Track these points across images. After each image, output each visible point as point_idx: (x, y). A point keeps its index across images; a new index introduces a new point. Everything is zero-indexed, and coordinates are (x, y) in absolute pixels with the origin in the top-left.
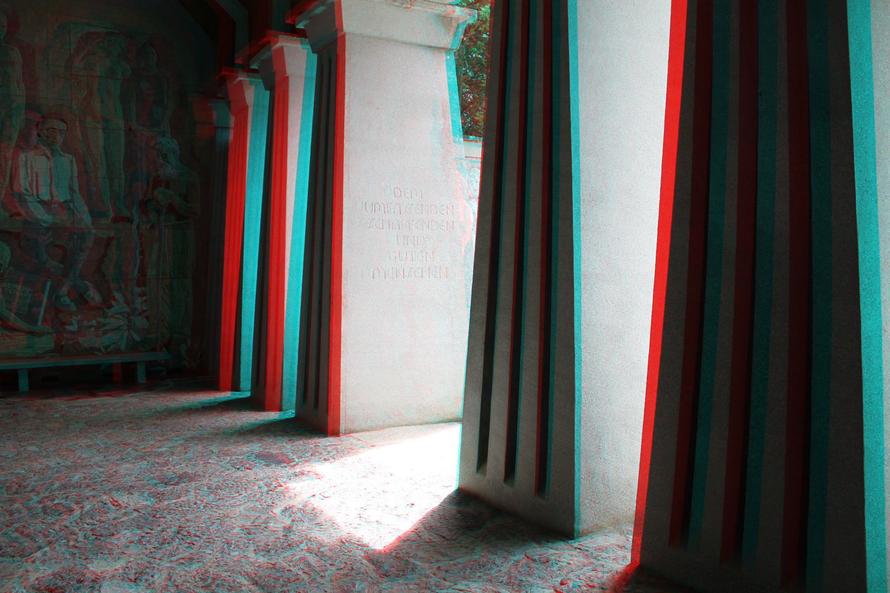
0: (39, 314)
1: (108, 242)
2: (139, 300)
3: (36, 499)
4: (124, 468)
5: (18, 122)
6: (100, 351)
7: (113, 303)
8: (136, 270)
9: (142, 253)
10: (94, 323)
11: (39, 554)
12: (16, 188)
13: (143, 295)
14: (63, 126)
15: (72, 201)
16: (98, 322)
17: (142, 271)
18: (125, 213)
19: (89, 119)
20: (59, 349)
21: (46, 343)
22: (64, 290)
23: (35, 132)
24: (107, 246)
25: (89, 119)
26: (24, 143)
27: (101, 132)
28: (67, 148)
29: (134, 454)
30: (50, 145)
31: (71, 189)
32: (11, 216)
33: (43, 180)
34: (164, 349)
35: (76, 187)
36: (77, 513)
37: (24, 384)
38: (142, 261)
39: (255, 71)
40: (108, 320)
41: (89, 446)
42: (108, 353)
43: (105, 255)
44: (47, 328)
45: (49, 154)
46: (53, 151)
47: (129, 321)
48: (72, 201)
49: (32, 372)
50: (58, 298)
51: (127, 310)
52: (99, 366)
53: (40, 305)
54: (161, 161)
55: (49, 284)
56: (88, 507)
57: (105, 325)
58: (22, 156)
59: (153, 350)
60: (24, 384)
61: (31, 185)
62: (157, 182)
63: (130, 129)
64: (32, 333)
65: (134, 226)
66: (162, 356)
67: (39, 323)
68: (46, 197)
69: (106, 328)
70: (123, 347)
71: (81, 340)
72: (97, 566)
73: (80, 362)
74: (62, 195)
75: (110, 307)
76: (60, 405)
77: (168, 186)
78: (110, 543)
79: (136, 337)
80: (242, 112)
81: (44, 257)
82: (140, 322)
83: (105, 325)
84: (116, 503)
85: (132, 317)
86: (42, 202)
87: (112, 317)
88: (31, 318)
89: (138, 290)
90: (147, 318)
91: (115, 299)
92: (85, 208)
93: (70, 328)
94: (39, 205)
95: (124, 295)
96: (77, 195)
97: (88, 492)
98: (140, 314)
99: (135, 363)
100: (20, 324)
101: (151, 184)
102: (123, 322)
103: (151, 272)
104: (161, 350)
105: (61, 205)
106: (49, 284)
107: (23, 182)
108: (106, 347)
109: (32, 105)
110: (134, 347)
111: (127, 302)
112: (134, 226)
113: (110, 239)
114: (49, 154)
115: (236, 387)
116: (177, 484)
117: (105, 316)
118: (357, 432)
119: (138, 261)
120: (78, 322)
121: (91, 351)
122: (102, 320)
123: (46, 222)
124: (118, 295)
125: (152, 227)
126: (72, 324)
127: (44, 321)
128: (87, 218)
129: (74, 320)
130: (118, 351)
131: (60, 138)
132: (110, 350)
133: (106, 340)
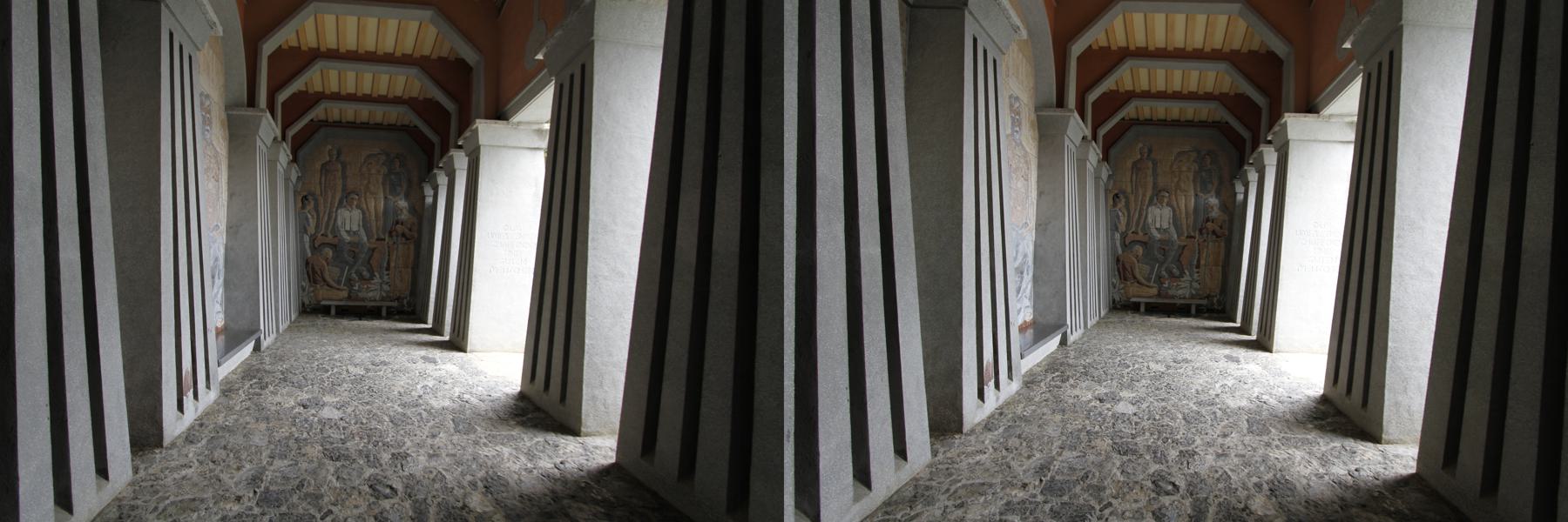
5: (338, 196)
26: (340, 204)
74: (355, 228)
109: (344, 188)
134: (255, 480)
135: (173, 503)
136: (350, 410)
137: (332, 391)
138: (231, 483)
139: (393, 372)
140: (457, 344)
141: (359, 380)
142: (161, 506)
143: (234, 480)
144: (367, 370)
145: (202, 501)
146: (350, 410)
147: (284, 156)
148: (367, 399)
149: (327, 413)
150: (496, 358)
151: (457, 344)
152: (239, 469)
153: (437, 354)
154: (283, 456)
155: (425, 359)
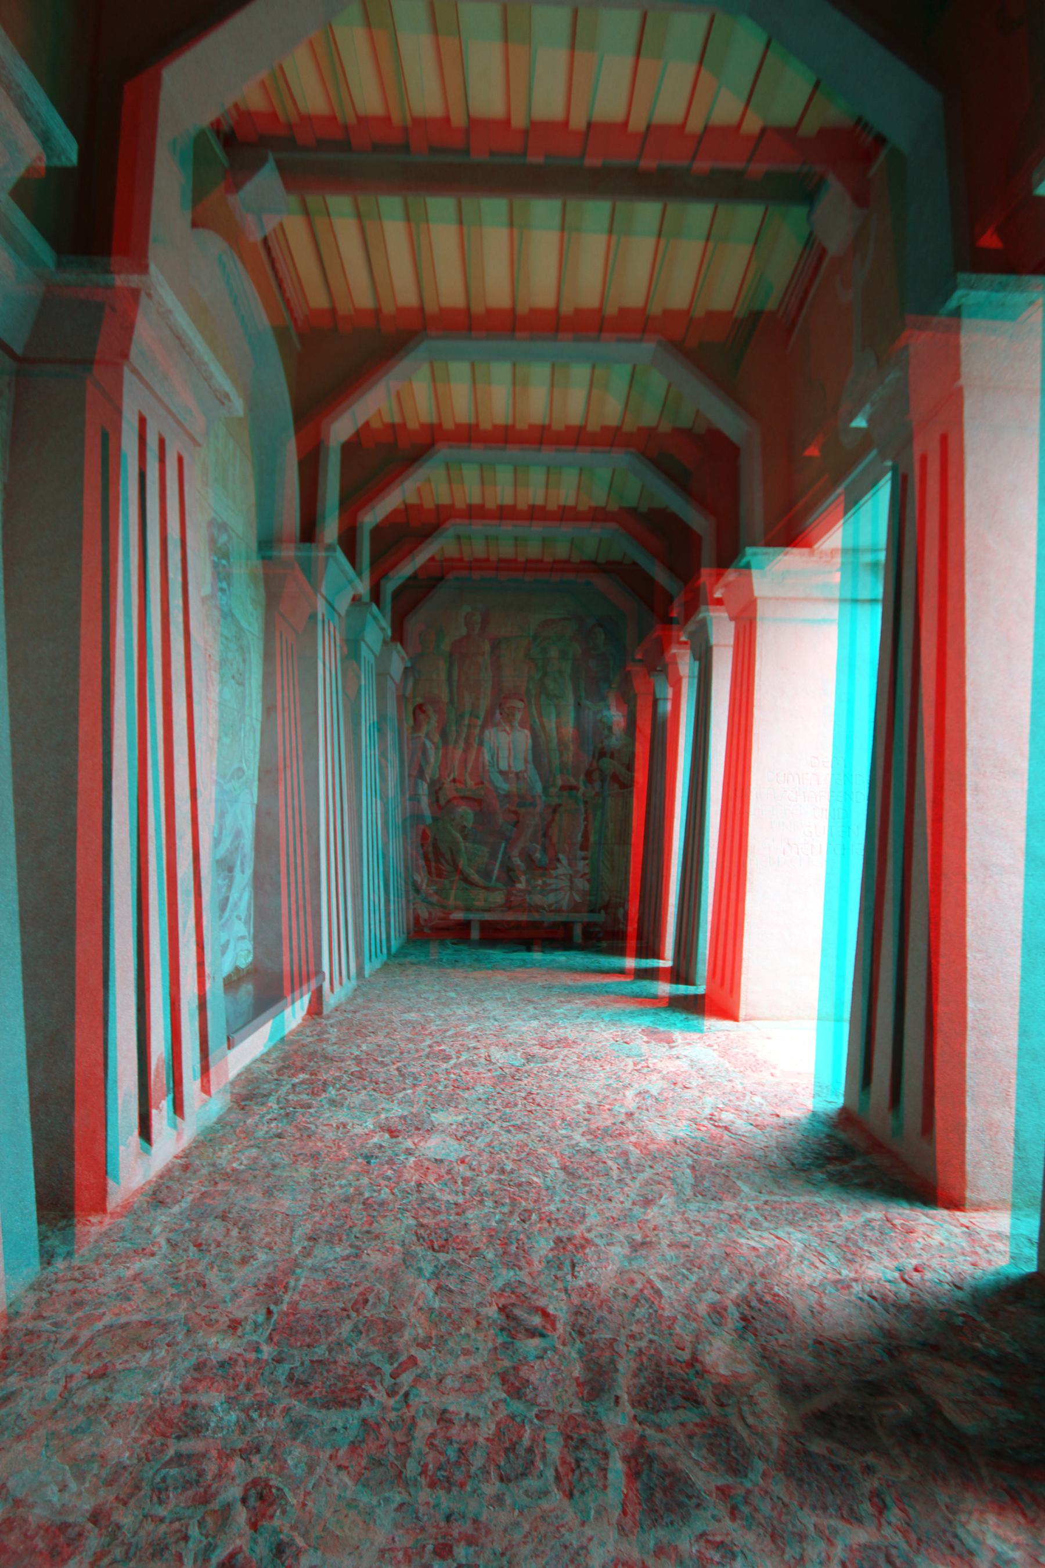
0: (493, 871)
1: (555, 810)
2: (581, 865)
3: (428, 1042)
4: (516, 1024)
5: (485, 703)
6: (544, 908)
7: (558, 865)
8: (580, 835)
9: (586, 819)
10: (540, 882)
11: (400, 1095)
12: (481, 760)
13: (585, 858)
14: (521, 705)
15: (526, 771)
16: (544, 882)
17: (586, 836)
18: (572, 781)
19: (543, 697)
20: (508, 906)
21: (498, 898)
22: (515, 852)
23: (498, 712)
24: (555, 811)
25: (543, 697)
26: (489, 721)
27: (553, 711)
28: (522, 725)
29: (532, 1011)
30: (510, 722)
31: (526, 761)
32: (476, 784)
33: (504, 753)
34: (603, 911)
35: (530, 758)
36: (452, 1062)
37: (475, 934)
38: (586, 827)
39: (685, 643)
40: (552, 881)
41: (498, 999)
42: (551, 911)
43: (553, 820)
44: (500, 885)
45: (508, 729)
46: (512, 727)
47: (571, 882)
48: (526, 771)
49: (484, 925)
50: (509, 858)
51: (571, 872)
52: (542, 923)
53: (494, 865)
54: (606, 732)
55: (503, 845)
56: (464, 1056)
57: (550, 884)
58: (487, 733)
59: (592, 911)
60: (475, 934)
61: (492, 758)
62: (602, 754)
63: (579, 704)
64: (486, 888)
65: (580, 794)
66: (600, 917)
67: (494, 878)
68: (503, 766)
69: (549, 888)
70: (565, 908)
71: (527, 897)
72: (441, 1118)
73: (524, 917)
74: (519, 766)
75: (556, 868)
76: (497, 955)
77: (612, 757)
78: (462, 1097)
79: (577, 898)
80: (677, 685)
81: (501, 821)
82: (582, 884)
83: (550, 884)
84: (488, 1059)
85: (576, 880)
86: (501, 772)
87: (556, 877)
88: (486, 874)
89: (580, 854)
90: (588, 881)
91: (558, 860)
92: (537, 777)
93: (519, 886)
94: (498, 775)
95: (569, 860)
96: (531, 766)
97: (473, 1044)
98: (582, 877)
99: (573, 923)
100: (476, 878)
101: (597, 754)
102: (567, 883)
103: (593, 838)
104: (599, 912)
105: (517, 774)
106: (503, 845)
107: (487, 757)
108: (550, 905)
110: (575, 908)
111: (570, 865)
112: (580, 794)
113: (559, 805)
114: (508, 729)
115: (658, 955)
116: (552, 1048)
117: (550, 876)
118: (759, 1019)
119: (582, 827)
120: (527, 881)
121: (537, 908)
122: (548, 881)
123: (503, 790)
124: (561, 856)
125: (597, 794)
126: (520, 882)
127: (498, 879)
128: (539, 787)
129: (523, 878)
130: (559, 911)
131: (518, 716)
132: (553, 908)
133: (551, 898)
134: (272, 1288)
135: (109, 1329)
136: (481, 1143)
137: (451, 1101)
138: (223, 1290)
139: (581, 1059)
140: (718, 1003)
141: (507, 1078)
142: (85, 1335)
143: (234, 1288)
144: (529, 1058)
145: (164, 1326)
146: (481, 1143)
147: (376, 630)
148: (519, 1116)
149: (433, 1146)
150: (783, 1043)
151: (718, 1003)
152: (244, 1261)
153: (676, 1024)
154: (333, 1238)
155: (651, 1033)
